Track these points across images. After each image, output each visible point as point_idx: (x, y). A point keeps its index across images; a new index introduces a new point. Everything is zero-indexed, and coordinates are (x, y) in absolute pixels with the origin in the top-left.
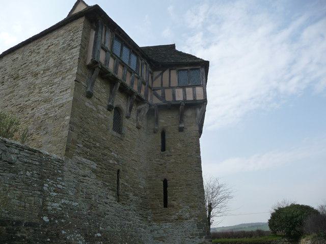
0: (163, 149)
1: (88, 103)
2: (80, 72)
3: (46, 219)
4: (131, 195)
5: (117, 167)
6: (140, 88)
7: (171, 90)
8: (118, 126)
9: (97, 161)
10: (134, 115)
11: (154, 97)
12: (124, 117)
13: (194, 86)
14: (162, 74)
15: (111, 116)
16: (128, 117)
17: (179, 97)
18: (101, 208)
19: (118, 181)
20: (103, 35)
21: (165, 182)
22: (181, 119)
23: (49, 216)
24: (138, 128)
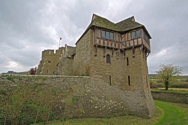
0: (128, 65)
1: (96, 58)
2: (92, 49)
3: (86, 95)
4: (116, 83)
5: (110, 75)
6: (115, 45)
7: (128, 42)
8: (109, 61)
9: (101, 75)
10: (115, 55)
12: (111, 57)
13: (137, 39)
14: (125, 35)
15: (105, 58)
16: (112, 57)
17: (132, 45)
18: (104, 89)
19: (110, 80)
20: (97, 33)
21: (129, 77)
23: (87, 94)
24: (117, 59)
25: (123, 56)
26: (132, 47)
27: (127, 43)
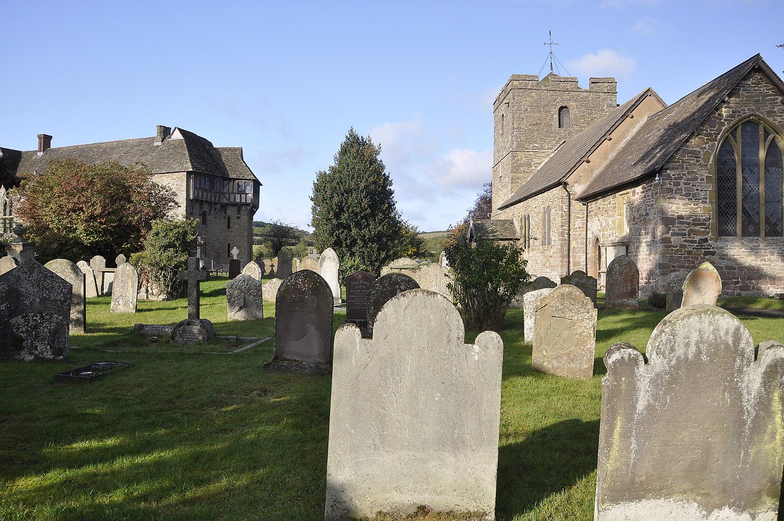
0: (229, 228)
11: (224, 199)
14: (229, 183)
16: (209, 215)
17: (238, 200)
21: (229, 245)
22: (239, 212)
25: (223, 214)
26: (238, 204)
27: (232, 196)
